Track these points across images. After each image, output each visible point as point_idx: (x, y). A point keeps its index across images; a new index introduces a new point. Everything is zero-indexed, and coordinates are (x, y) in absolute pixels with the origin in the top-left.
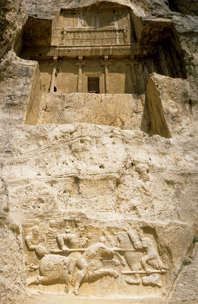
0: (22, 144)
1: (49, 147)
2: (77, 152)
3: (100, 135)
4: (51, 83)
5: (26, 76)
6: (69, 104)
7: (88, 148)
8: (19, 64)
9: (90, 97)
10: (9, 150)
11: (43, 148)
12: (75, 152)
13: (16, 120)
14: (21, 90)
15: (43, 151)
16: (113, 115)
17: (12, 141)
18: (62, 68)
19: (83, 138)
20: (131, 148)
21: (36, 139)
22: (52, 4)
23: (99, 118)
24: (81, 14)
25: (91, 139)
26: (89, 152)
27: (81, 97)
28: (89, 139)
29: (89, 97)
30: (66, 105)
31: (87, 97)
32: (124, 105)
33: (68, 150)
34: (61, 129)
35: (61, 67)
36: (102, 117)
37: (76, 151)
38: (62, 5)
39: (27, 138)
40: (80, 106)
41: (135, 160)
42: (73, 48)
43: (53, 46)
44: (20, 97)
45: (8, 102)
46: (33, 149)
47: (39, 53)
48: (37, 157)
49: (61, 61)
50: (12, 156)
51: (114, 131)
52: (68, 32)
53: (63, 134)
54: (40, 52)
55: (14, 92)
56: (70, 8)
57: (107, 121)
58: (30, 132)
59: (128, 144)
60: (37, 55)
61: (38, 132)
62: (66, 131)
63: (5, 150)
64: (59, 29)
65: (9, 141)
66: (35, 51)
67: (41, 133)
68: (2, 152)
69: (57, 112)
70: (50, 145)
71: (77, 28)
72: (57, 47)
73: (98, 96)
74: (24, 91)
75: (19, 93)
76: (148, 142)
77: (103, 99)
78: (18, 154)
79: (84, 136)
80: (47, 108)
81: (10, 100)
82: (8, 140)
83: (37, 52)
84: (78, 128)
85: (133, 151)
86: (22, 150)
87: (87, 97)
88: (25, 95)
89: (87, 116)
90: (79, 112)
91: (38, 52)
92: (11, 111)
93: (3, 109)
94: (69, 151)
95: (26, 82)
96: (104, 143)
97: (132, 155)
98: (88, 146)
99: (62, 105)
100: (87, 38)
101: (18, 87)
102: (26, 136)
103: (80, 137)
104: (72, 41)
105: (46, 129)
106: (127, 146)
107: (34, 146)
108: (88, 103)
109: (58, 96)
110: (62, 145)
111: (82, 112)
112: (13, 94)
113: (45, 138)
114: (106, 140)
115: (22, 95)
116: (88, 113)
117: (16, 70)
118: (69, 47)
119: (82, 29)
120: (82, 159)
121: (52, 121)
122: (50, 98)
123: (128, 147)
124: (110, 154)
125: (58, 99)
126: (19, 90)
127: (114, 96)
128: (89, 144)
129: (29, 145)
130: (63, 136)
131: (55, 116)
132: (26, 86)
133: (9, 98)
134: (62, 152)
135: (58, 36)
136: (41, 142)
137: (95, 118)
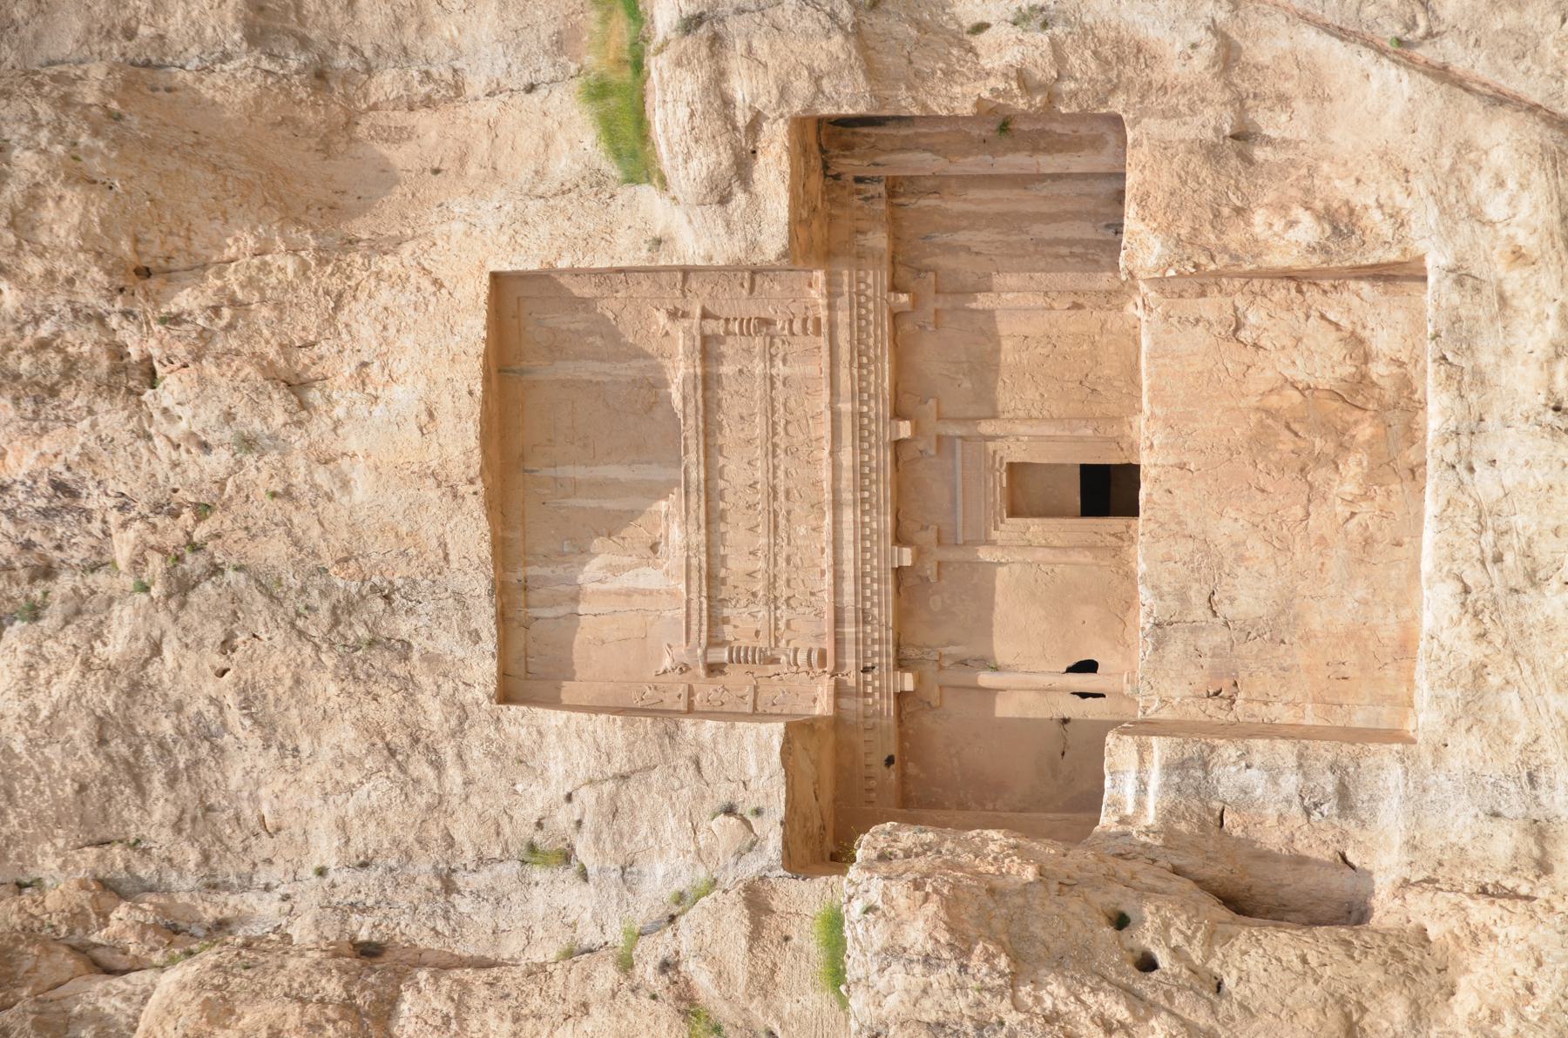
0: (1499, 741)
1: (1515, 655)
2: (1534, 571)
3: (1471, 504)
4: (1049, 689)
5: (1205, 765)
6: (1198, 599)
7: (1523, 540)
8: (1140, 804)
9: (1160, 513)
10: (1525, 778)
11: (1514, 675)
12: (1533, 578)
13: (1406, 773)
14: (1274, 774)
15: (1527, 673)
16: (1254, 418)
17: (1494, 771)
18: (950, 643)
19: (1489, 555)
20: (1497, 409)
21: (1481, 698)
22: (420, 768)
23: (1264, 481)
24: (533, 571)
25: (1490, 532)
26: (1536, 538)
27: (1160, 549)
28: (1489, 537)
29: (1163, 516)
30: (1200, 612)
31: (1162, 525)
32: (1201, 373)
33: (1525, 599)
34: (1445, 623)
35: (945, 651)
36: (1260, 466)
37: (1532, 577)
38: (450, 701)
39: (1475, 728)
40: (1207, 554)
41: (1542, 399)
42: (848, 599)
43: (836, 706)
44: (1305, 774)
45: (1335, 811)
46: (1516, 704)
47: (878, 768)
48: (1550, 690)
49: (911, 652)
50: (1547, 765)
51: (1450, 458)
52: (714, 641)
53: (1469, 616)
54: (868, 766)
55: (1289, 802)
56: (489, 644)
57: (1280, 446)
58: (1455, 720)
59: (1485, 416)
60: (893, 776)
61: (1452, 694)
62: (1457, 607)
63: (1527, 789)
64: (682, 689)
65: (1493, 784)
66: (869, 790)
67: (1463, 682)
68: (1537, 797)
69: (1242, 649)
70: (1508, 652)
71: (682, 587)
72: (837, 682)
73: (1156, 480)
74: (1280, 763)
75: (1290, 782)
76: (1469, 347)
77: (1172, 459)
78: (1535, 747)
79: (1482, 551)
80: (1216, 694)
81: (1325, 808)
82: (1489, 787)
83: (873, 783)
84: (1450, 571)
85: (1509, 402)
86: (1520, 738)
87: (1162, 525)
88: (1301, 756)
89: (1255, 526)
90: (1240, 558)
91: (868, 778)
92: (1366, 798)
93: (1363, 824)
94: (1530, 596)
95: (1234, 763)
96: (1501, 494)
97: (1525, 407)
98: (1515, 541)
99: (1203, 629)
100: (760, 530)
101: (1259, 792)
102: (1469, 730)
103: (1483, 563)
104: (784, 612)
105: (1446, 669)
106: (1491, 422)
107: (1505, 703)
108: (1191, 523)
109: (1156, 649)
110: (1509, 619)
111: (1235, 545)
112: (1297, 800)
113: (1479, 672)
114: (1485, 484)
115: (1300, 766)
116: (1241, 522)
117: (1187, 808)
118: (838, 621)
119: (688, 566)
120: (1558, 556)
121: (1284, 669)
122: (1166, 684)
123: (1497, 416)
124: (1540, 479)
125: (1174, 650)
126: (1276, 784)
127: (1158, 411)
128: (1507, 537)
129: (1500, 720)
130: (1476, 615)
131: (1257, 656)
132: (1257, 759)
133: (1316, 813)
134: (1531, 617)
135: (748, 690)
136: (1494, 680)
137: (1263, 491)
